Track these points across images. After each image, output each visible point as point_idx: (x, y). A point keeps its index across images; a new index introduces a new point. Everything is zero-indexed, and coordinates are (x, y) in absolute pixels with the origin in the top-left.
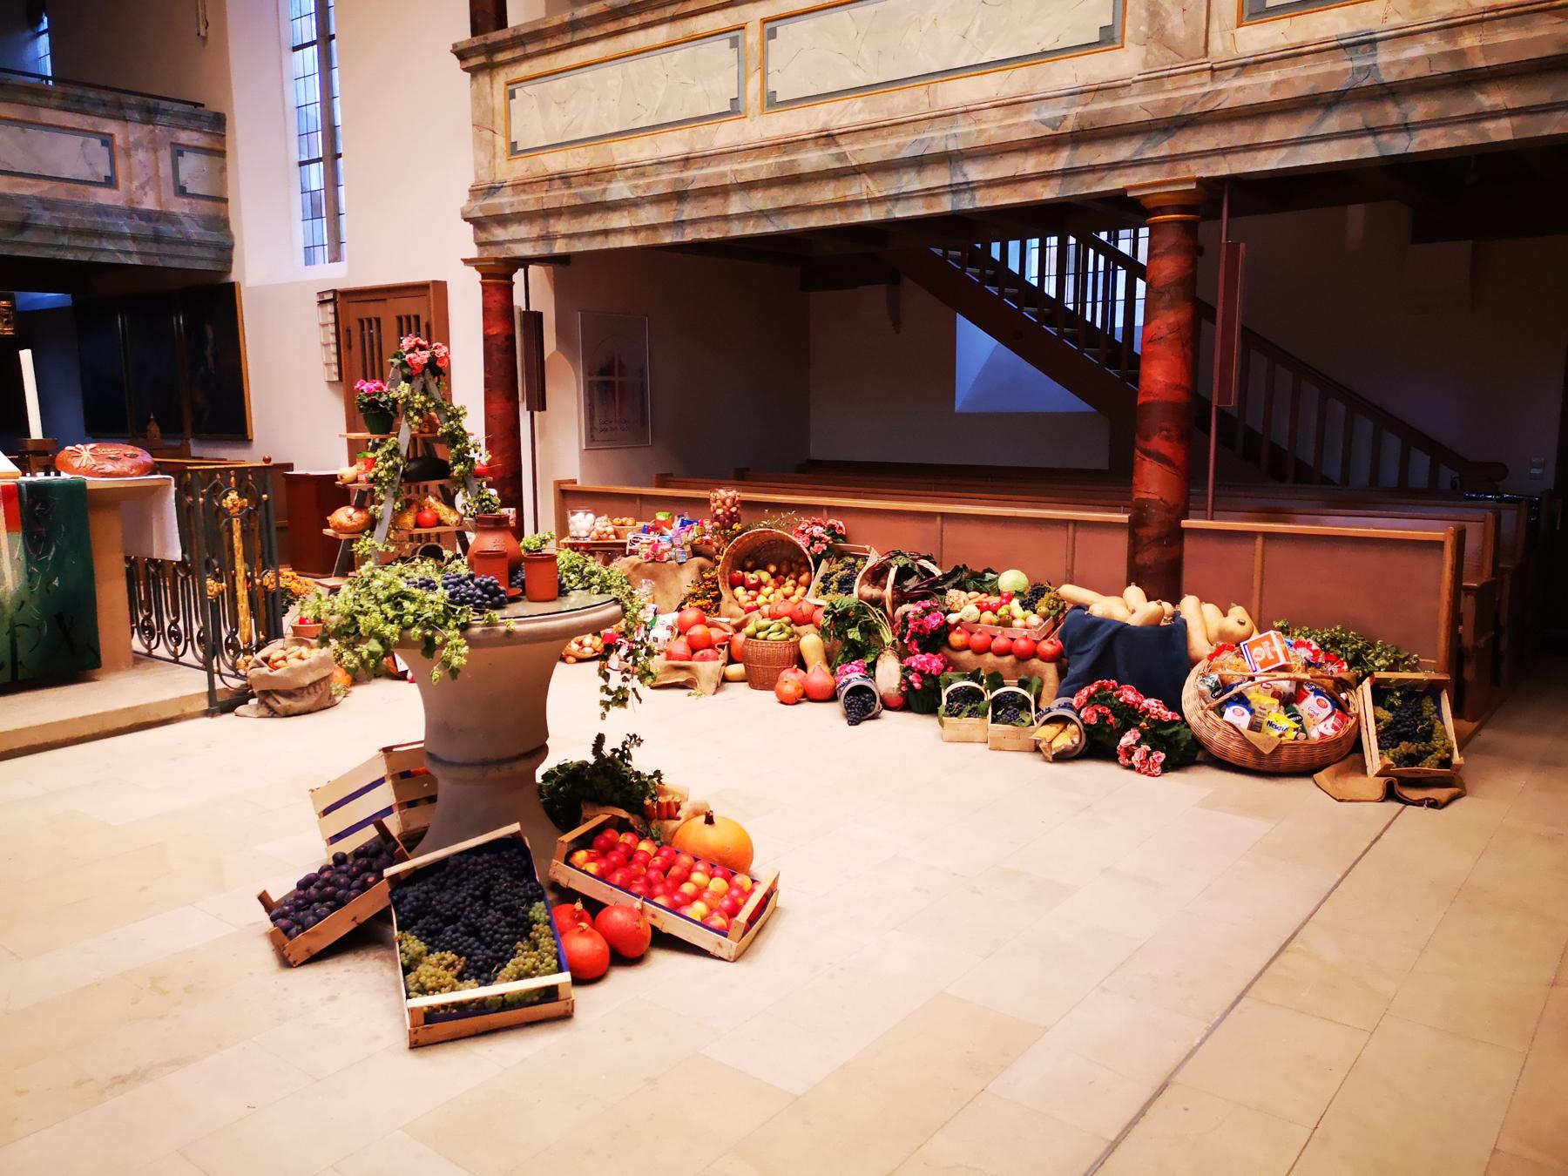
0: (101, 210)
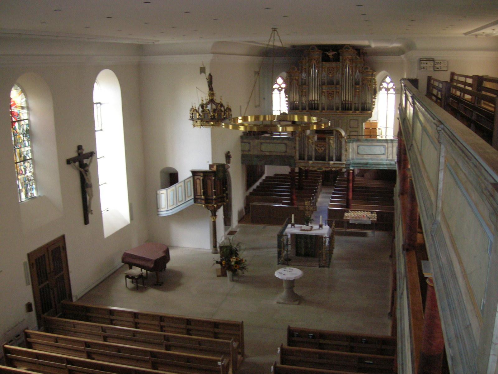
0: (382, 160)
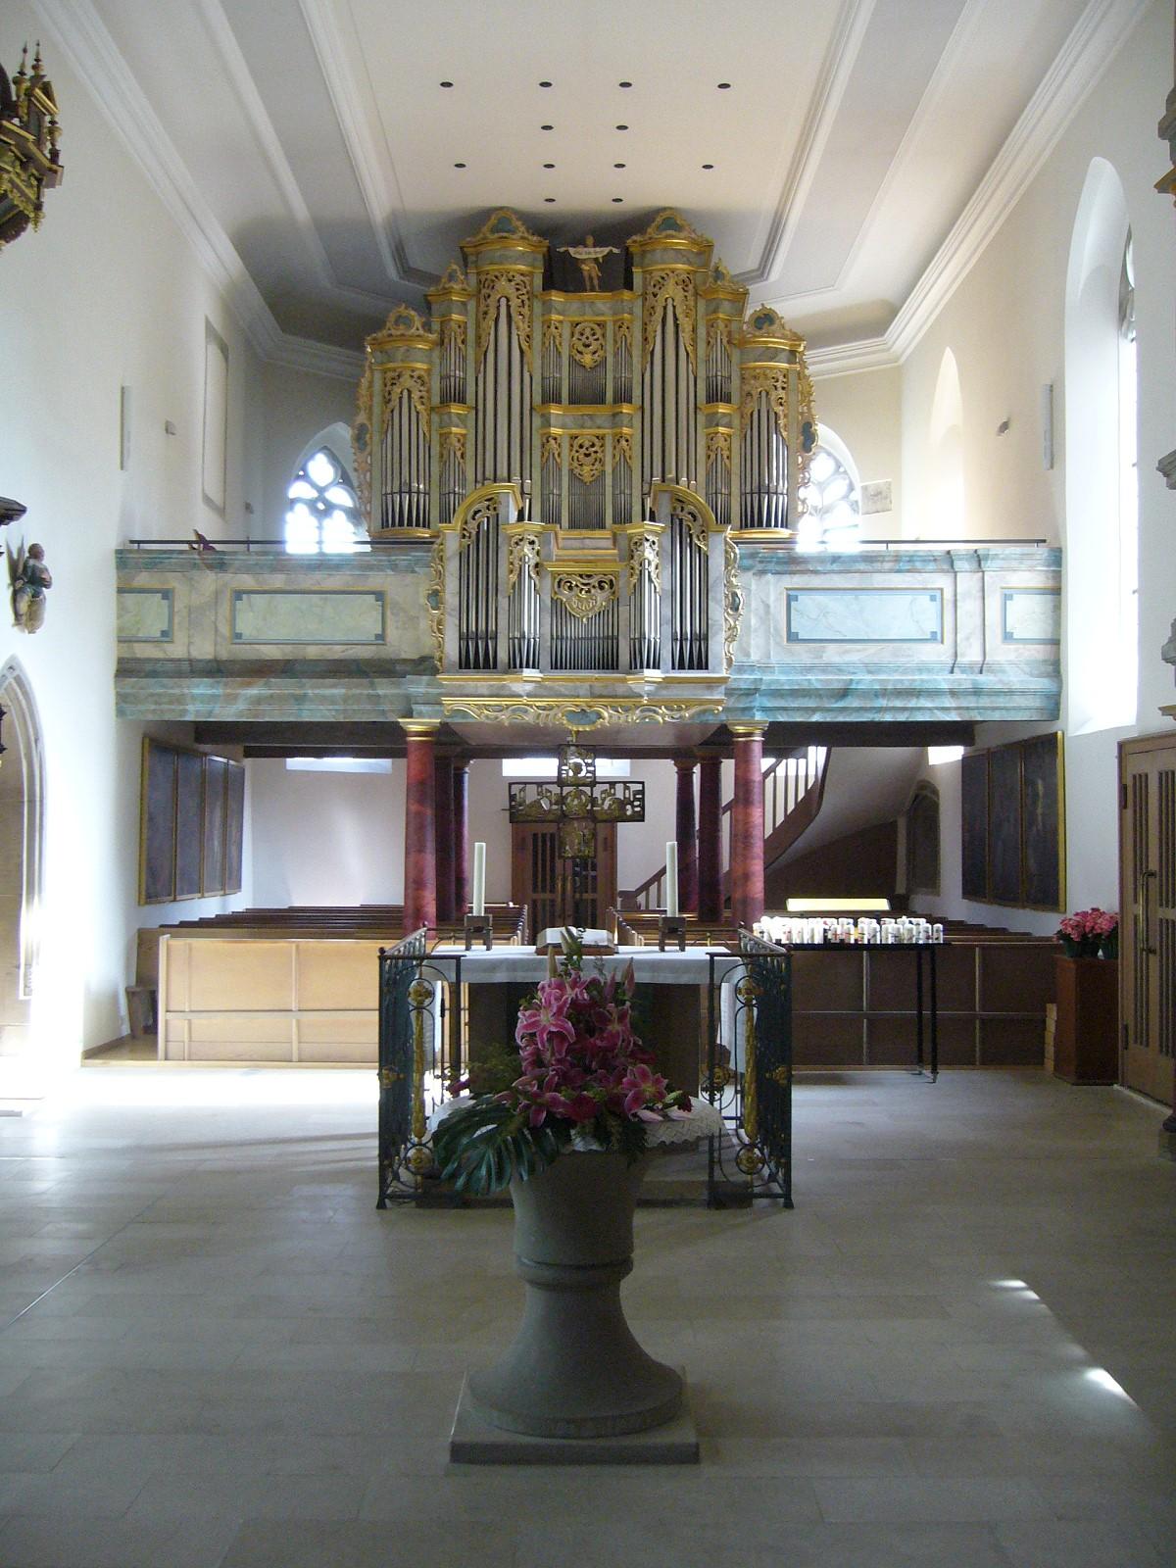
0: (921, 669)
